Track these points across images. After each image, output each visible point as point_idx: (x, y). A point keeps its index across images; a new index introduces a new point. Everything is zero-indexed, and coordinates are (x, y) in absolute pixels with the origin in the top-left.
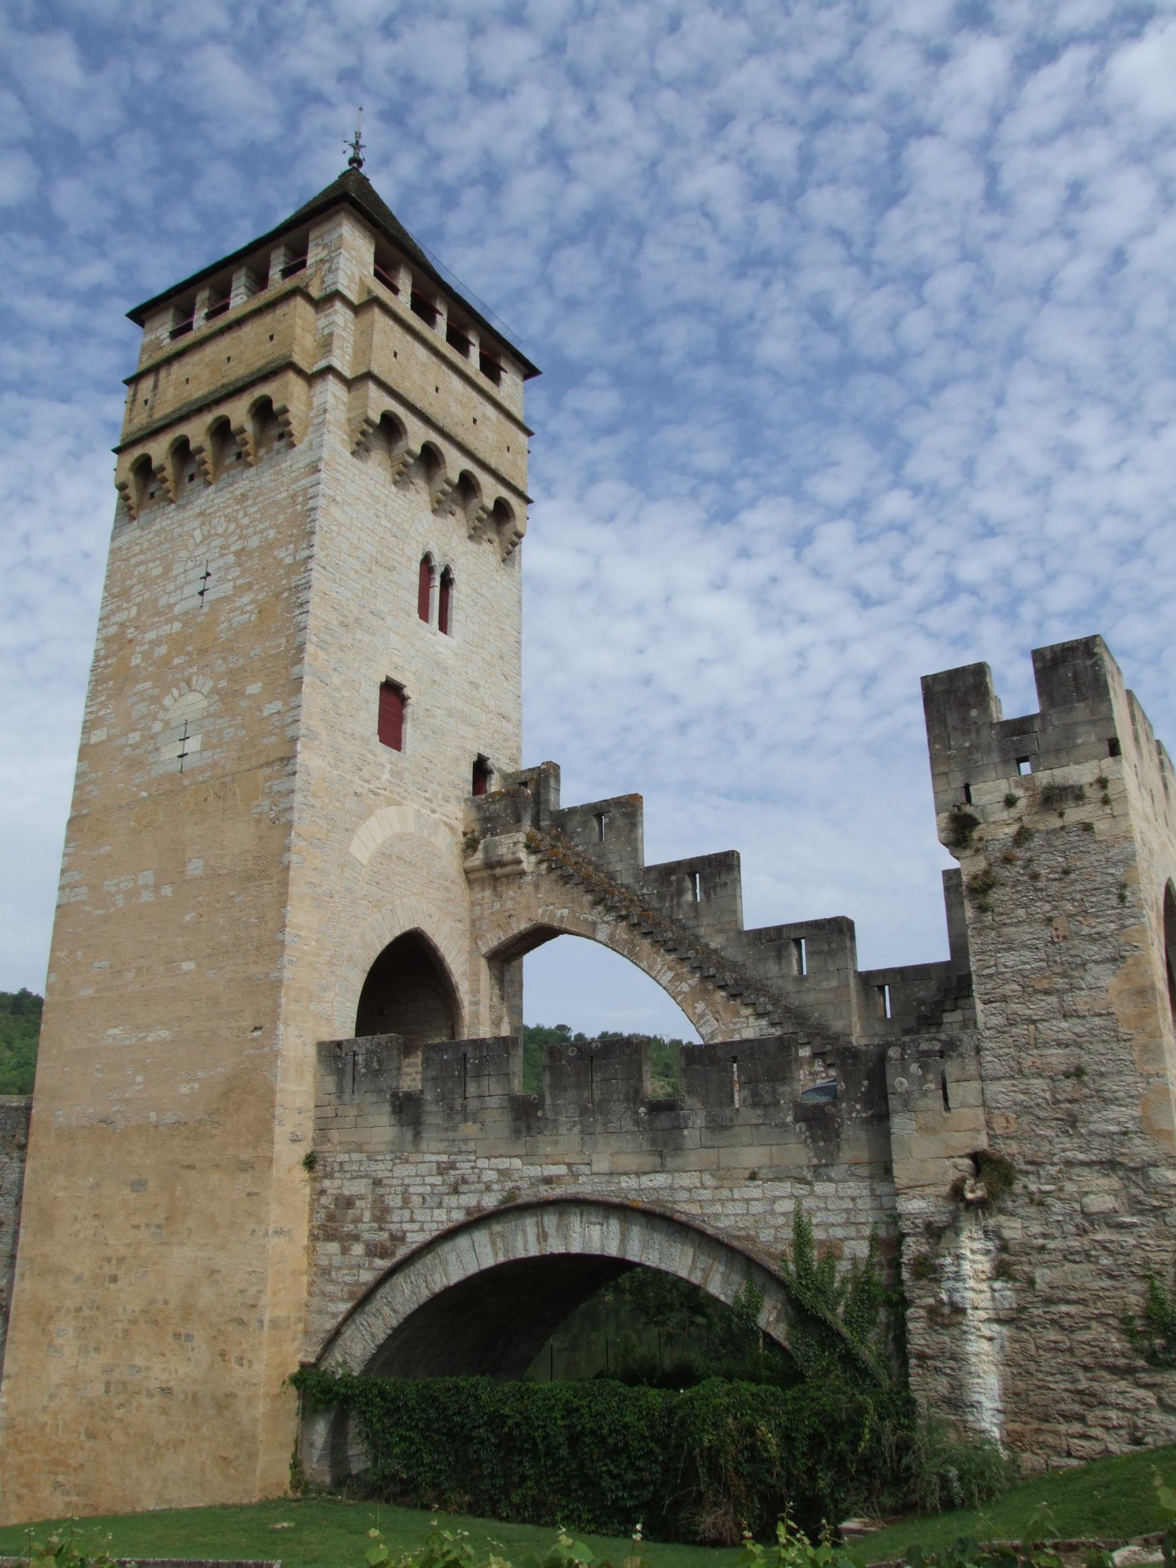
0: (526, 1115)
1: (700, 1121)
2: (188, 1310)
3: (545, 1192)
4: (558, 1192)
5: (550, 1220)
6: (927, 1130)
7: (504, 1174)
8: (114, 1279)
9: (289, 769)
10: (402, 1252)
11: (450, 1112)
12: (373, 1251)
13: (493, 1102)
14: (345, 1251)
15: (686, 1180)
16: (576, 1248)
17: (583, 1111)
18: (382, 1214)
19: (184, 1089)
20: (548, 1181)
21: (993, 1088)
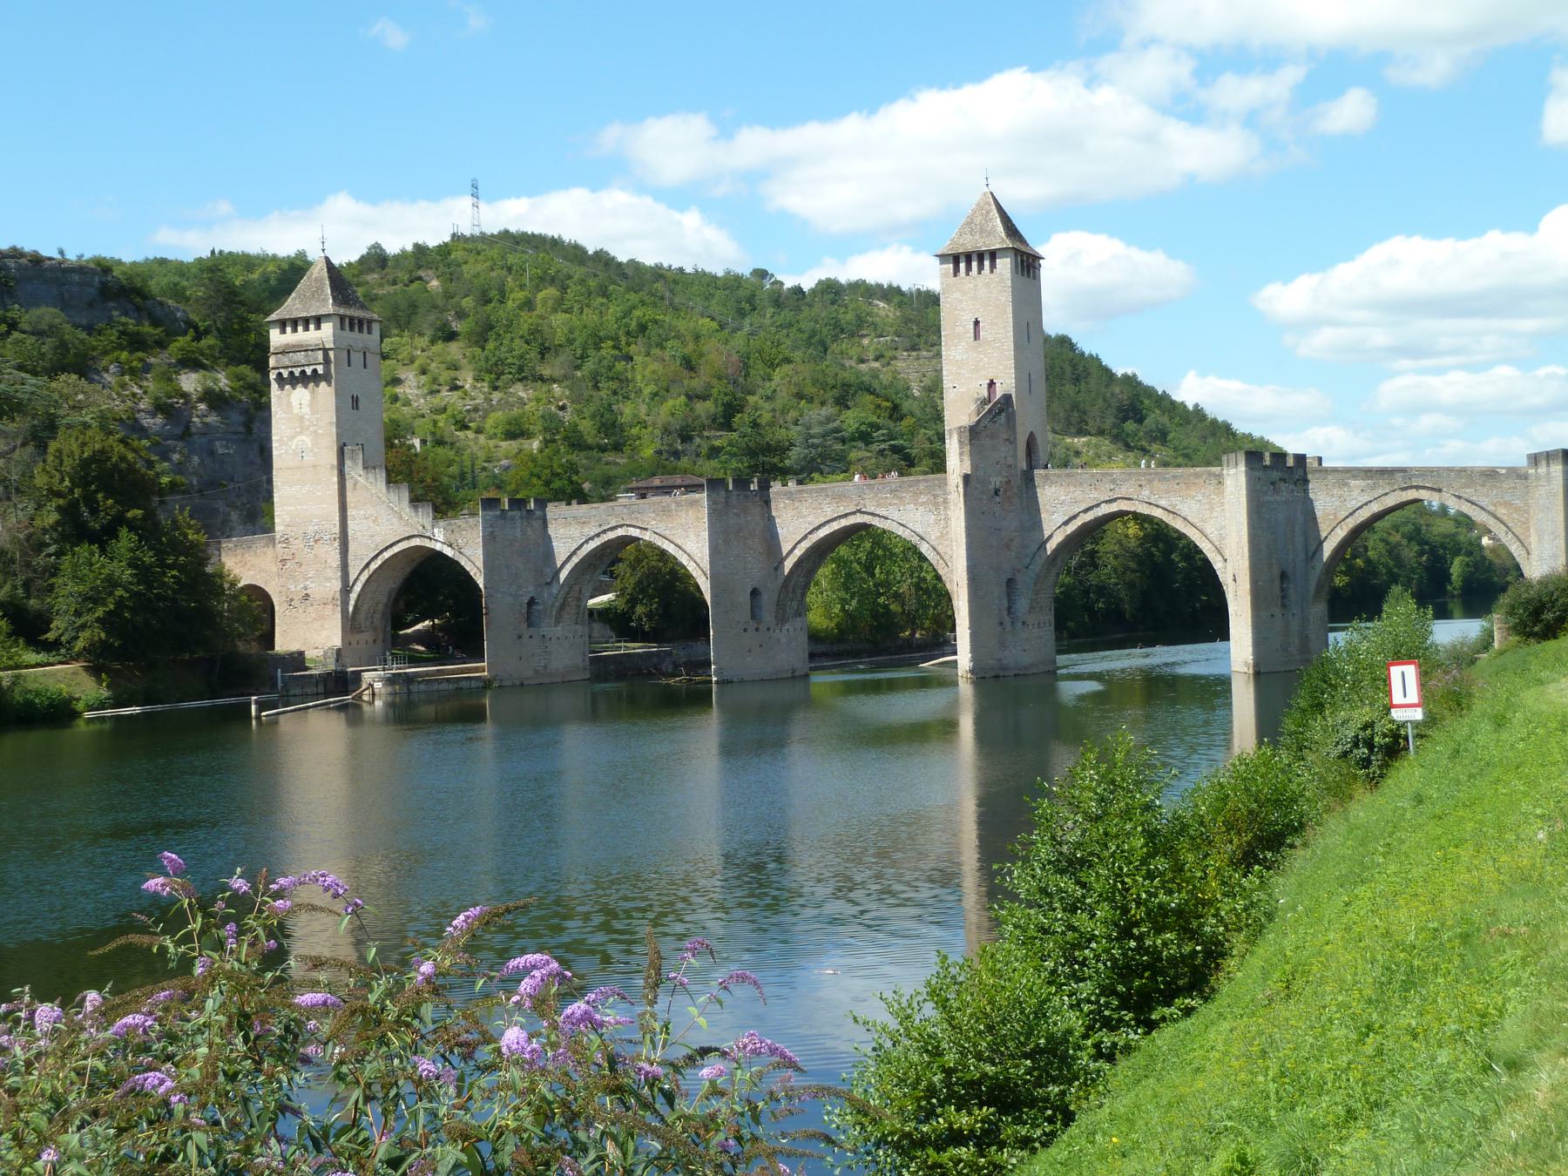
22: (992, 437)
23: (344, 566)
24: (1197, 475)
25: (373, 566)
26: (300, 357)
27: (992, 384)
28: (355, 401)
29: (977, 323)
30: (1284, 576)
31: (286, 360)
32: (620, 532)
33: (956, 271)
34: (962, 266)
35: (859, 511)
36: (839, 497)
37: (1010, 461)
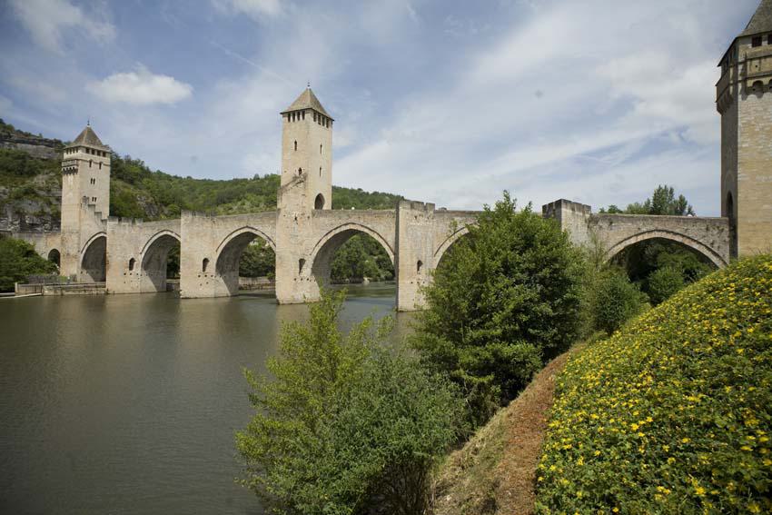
22: (295, 192)
23: (79, 244)
24: (385, 213)
25: (89, 243)
26: (70, 163)
27: (300, 170)
28: (93, 181)
29: (296, 143)
30: (419, 263)
31: (66, 164)
32: (165, 233)
33: (289, 120)
34: (291, 118)
35: (247, 227)
36: (240, 220)
37: (304, 205)
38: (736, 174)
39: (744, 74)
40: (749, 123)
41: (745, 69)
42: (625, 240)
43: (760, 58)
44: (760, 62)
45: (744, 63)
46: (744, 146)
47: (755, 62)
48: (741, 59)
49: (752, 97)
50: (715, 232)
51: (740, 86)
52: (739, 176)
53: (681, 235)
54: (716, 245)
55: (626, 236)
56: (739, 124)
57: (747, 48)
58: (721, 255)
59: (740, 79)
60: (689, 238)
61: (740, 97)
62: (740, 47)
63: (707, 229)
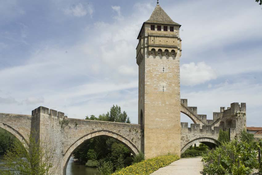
0: (201, 131)
1: (216, 132)
2: (171, 146)
3: (203, 137)
4: (204, 137)
5: (203, 139)
6: (233, 134)
7: (199, 135)
8: (160, 144)
9: (179, 95)
10: (189, 141)
11: (194, 130)
12: (186, 141)
13: (198, 129)
14: (183, 141)
15: (215, 136)
16: (206, 141)
17: (207, 131)
18: (187, 138)
19: (168, 126)
20: (203, 136)
21: (237, 132)
38: (144, 99)
39: (147, 43)
40: (150, 71)
41: (148, 41)
42: (85, 136)
43: (154, 36)
44: (154, 39)
45: (148, 37)
46: (148, 83)
47: (152, 38)
48: (146, 35)
49: (151, 57)
50: (134, 132)
51: (146, 49)
52: (145, 100)
53: (116, 134)
54: (134, 141)
55: (85, 134)
56: (145, 71)
57: (149, 30)
58: (137, 147)
59: (146, 45)
60: (120, 136)
61: (146, 56)
62: (146, 28)
63: (130, 131)
